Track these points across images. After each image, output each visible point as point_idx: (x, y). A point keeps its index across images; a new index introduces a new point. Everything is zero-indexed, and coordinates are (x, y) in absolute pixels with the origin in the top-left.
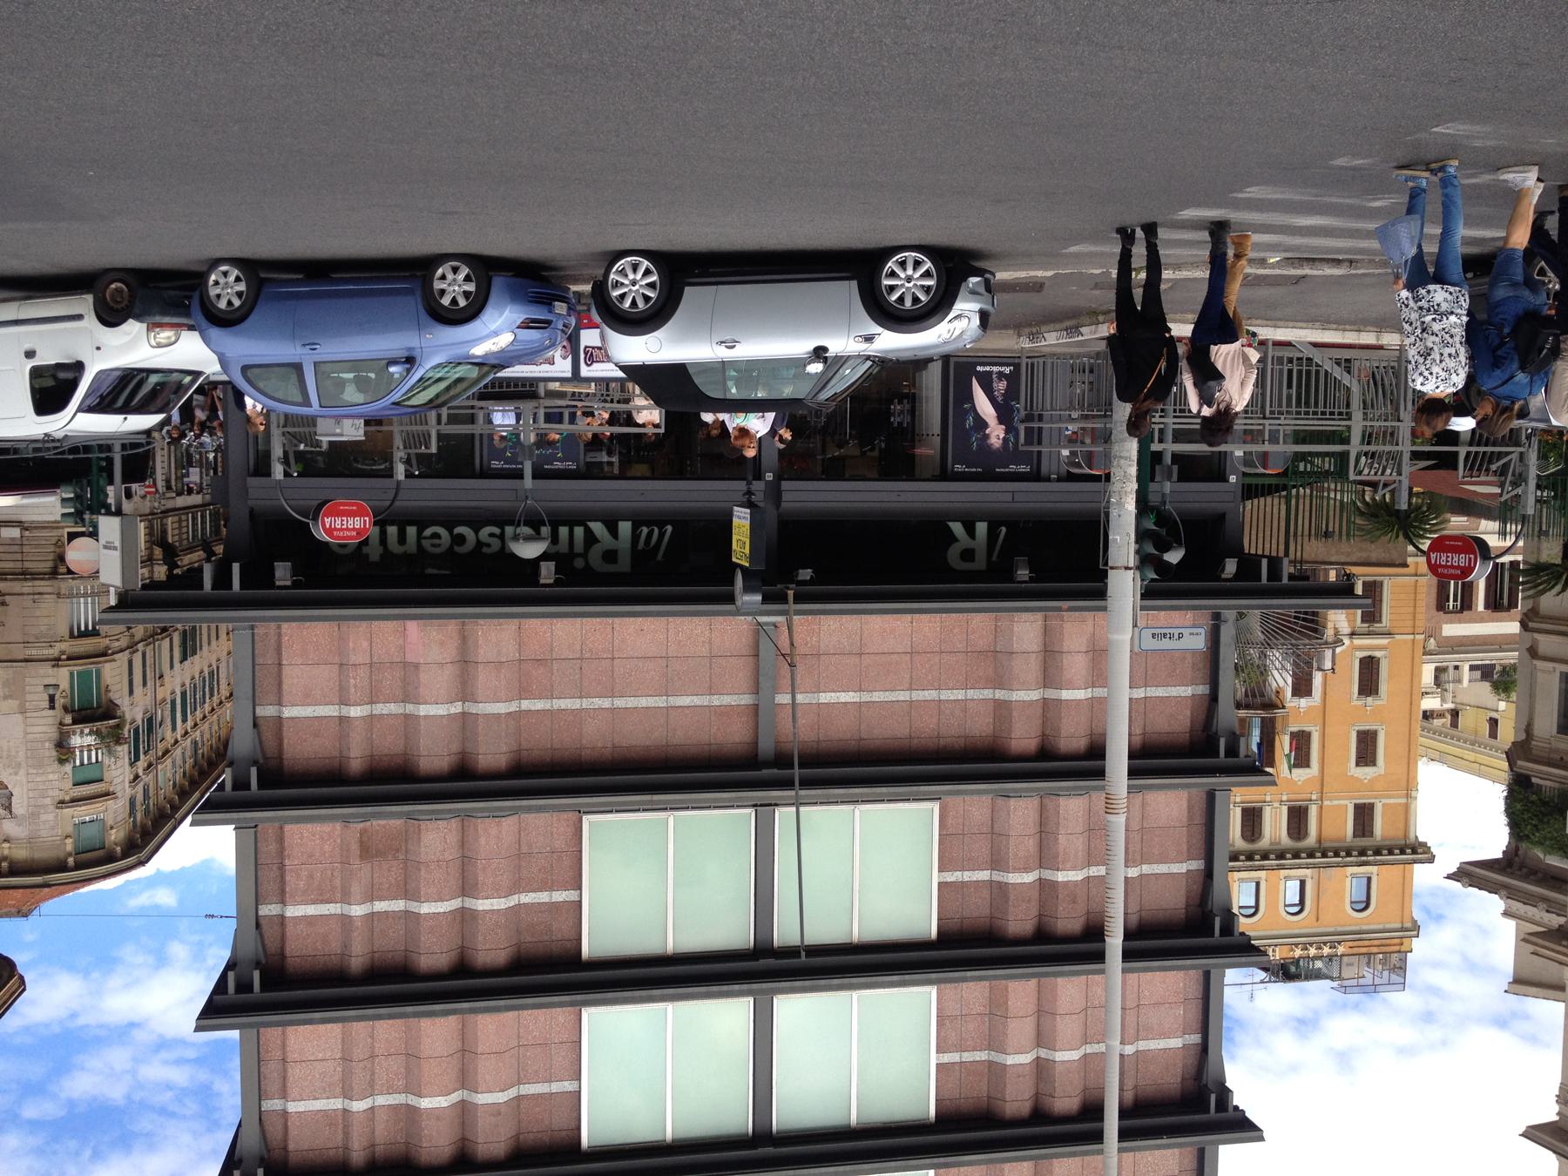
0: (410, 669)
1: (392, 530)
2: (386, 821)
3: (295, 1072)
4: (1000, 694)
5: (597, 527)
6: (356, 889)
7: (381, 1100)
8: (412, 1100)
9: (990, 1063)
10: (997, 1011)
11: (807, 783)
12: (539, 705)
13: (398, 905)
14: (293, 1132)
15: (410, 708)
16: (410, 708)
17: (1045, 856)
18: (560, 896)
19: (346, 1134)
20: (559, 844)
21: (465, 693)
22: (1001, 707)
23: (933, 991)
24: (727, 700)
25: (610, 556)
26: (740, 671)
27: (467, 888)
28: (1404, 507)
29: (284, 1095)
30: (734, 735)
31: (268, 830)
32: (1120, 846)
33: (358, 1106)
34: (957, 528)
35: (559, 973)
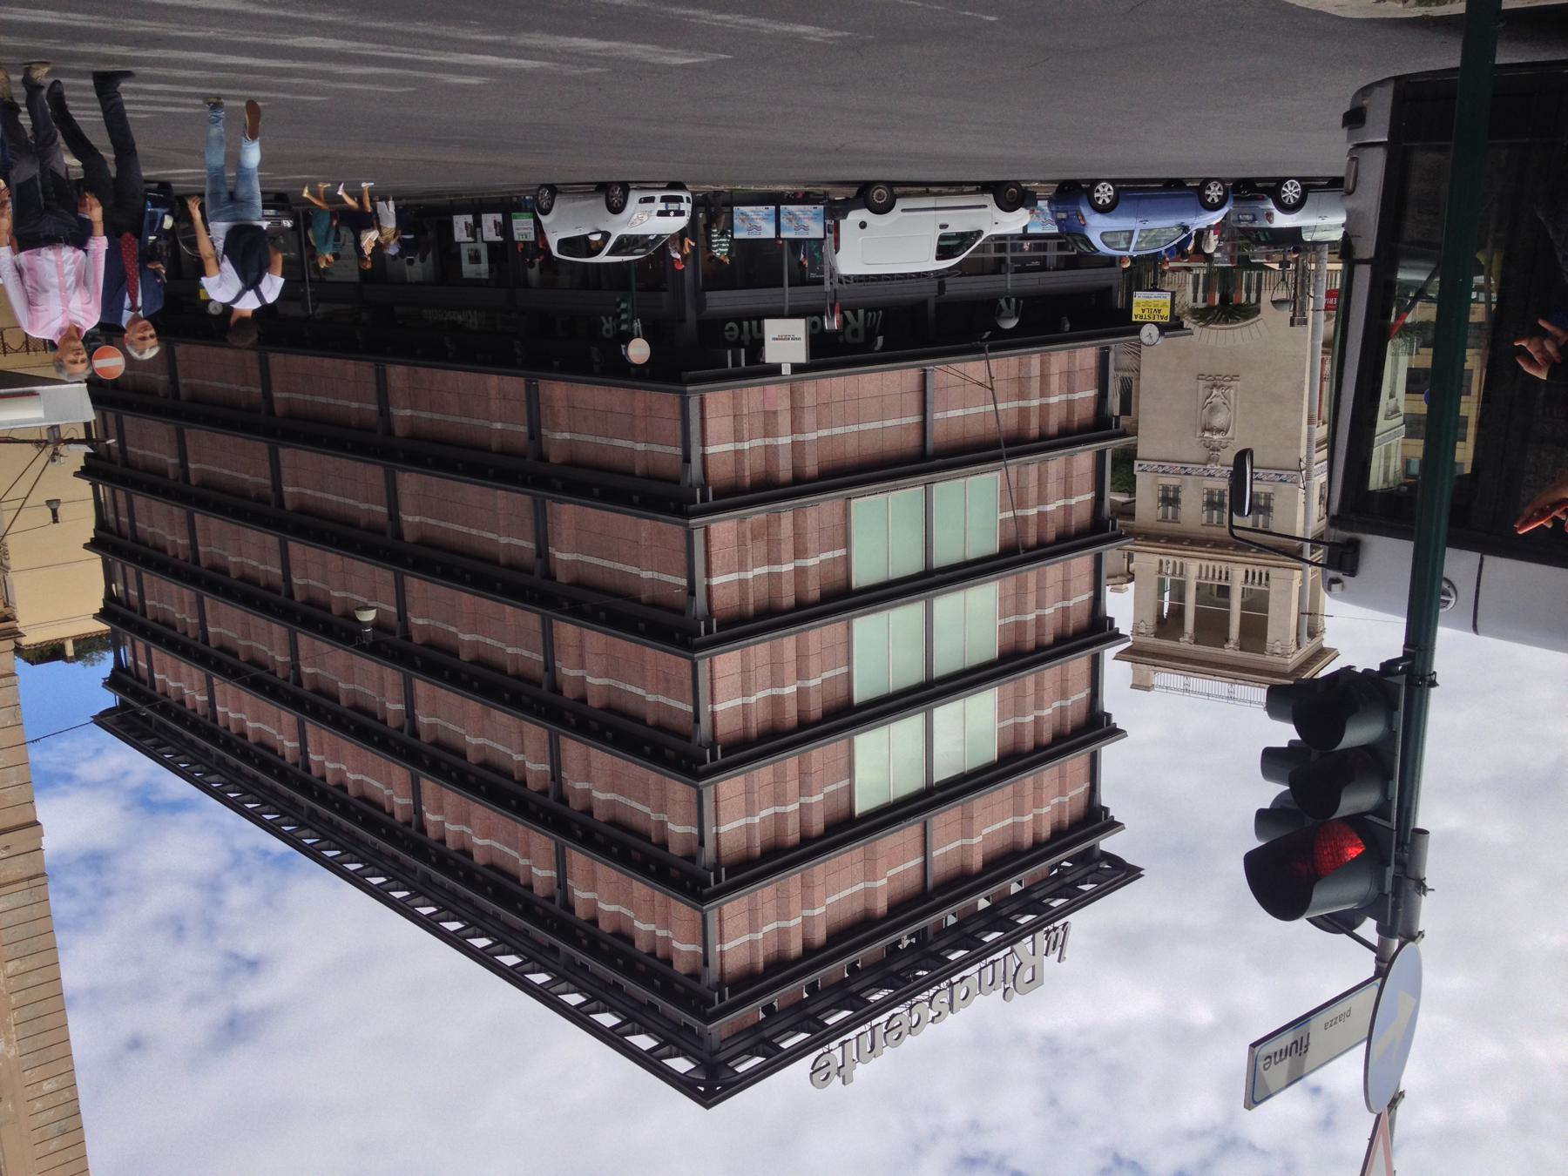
0: (770, 416)
1: (754, 323)
2: (757, 516)
3: (719, 685)
4: (1022, 404)
5: (848, 314)
6: (750, 561)
7: (761, 695)
8: (776, 691)
9: (1017, 622)
10: (1021, 591)
11: (1011, 456)
12: (824, 433)
13: (764, 570)
14: (719, 723)
15: (769, 441)
16: (769, 441)
17: (1042, 500)
18: (840, 553)
19: (746, 718)
20: (837, 521)
21: (796, 428)
22: (1023, 413)
23: (997, 584)
24: (905, 421)
25: (855, 333)
26: (913, 400)
27: (799, 553)
28: (1402, 276)
29: (713, 702)
30: (911, 441)
31: (1013, 470)
32: (1065, 486)
33: (753, 699)
34: (1003, 302)
35: (844, 599)
